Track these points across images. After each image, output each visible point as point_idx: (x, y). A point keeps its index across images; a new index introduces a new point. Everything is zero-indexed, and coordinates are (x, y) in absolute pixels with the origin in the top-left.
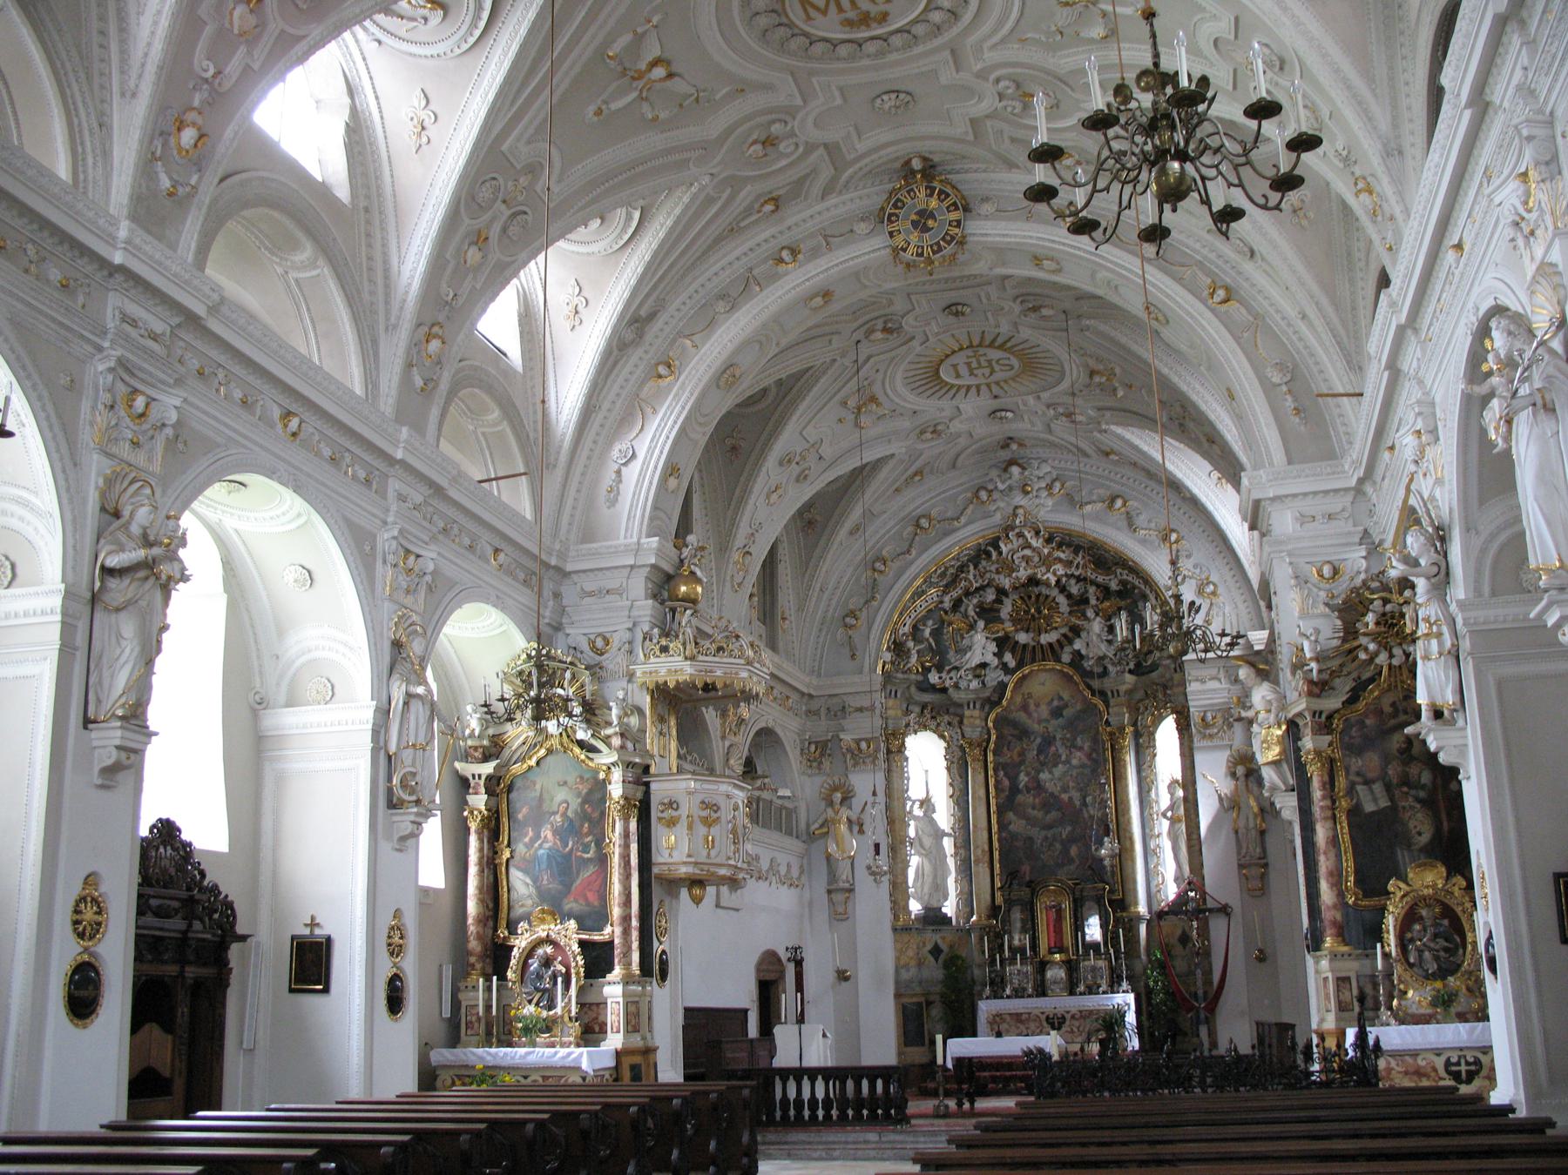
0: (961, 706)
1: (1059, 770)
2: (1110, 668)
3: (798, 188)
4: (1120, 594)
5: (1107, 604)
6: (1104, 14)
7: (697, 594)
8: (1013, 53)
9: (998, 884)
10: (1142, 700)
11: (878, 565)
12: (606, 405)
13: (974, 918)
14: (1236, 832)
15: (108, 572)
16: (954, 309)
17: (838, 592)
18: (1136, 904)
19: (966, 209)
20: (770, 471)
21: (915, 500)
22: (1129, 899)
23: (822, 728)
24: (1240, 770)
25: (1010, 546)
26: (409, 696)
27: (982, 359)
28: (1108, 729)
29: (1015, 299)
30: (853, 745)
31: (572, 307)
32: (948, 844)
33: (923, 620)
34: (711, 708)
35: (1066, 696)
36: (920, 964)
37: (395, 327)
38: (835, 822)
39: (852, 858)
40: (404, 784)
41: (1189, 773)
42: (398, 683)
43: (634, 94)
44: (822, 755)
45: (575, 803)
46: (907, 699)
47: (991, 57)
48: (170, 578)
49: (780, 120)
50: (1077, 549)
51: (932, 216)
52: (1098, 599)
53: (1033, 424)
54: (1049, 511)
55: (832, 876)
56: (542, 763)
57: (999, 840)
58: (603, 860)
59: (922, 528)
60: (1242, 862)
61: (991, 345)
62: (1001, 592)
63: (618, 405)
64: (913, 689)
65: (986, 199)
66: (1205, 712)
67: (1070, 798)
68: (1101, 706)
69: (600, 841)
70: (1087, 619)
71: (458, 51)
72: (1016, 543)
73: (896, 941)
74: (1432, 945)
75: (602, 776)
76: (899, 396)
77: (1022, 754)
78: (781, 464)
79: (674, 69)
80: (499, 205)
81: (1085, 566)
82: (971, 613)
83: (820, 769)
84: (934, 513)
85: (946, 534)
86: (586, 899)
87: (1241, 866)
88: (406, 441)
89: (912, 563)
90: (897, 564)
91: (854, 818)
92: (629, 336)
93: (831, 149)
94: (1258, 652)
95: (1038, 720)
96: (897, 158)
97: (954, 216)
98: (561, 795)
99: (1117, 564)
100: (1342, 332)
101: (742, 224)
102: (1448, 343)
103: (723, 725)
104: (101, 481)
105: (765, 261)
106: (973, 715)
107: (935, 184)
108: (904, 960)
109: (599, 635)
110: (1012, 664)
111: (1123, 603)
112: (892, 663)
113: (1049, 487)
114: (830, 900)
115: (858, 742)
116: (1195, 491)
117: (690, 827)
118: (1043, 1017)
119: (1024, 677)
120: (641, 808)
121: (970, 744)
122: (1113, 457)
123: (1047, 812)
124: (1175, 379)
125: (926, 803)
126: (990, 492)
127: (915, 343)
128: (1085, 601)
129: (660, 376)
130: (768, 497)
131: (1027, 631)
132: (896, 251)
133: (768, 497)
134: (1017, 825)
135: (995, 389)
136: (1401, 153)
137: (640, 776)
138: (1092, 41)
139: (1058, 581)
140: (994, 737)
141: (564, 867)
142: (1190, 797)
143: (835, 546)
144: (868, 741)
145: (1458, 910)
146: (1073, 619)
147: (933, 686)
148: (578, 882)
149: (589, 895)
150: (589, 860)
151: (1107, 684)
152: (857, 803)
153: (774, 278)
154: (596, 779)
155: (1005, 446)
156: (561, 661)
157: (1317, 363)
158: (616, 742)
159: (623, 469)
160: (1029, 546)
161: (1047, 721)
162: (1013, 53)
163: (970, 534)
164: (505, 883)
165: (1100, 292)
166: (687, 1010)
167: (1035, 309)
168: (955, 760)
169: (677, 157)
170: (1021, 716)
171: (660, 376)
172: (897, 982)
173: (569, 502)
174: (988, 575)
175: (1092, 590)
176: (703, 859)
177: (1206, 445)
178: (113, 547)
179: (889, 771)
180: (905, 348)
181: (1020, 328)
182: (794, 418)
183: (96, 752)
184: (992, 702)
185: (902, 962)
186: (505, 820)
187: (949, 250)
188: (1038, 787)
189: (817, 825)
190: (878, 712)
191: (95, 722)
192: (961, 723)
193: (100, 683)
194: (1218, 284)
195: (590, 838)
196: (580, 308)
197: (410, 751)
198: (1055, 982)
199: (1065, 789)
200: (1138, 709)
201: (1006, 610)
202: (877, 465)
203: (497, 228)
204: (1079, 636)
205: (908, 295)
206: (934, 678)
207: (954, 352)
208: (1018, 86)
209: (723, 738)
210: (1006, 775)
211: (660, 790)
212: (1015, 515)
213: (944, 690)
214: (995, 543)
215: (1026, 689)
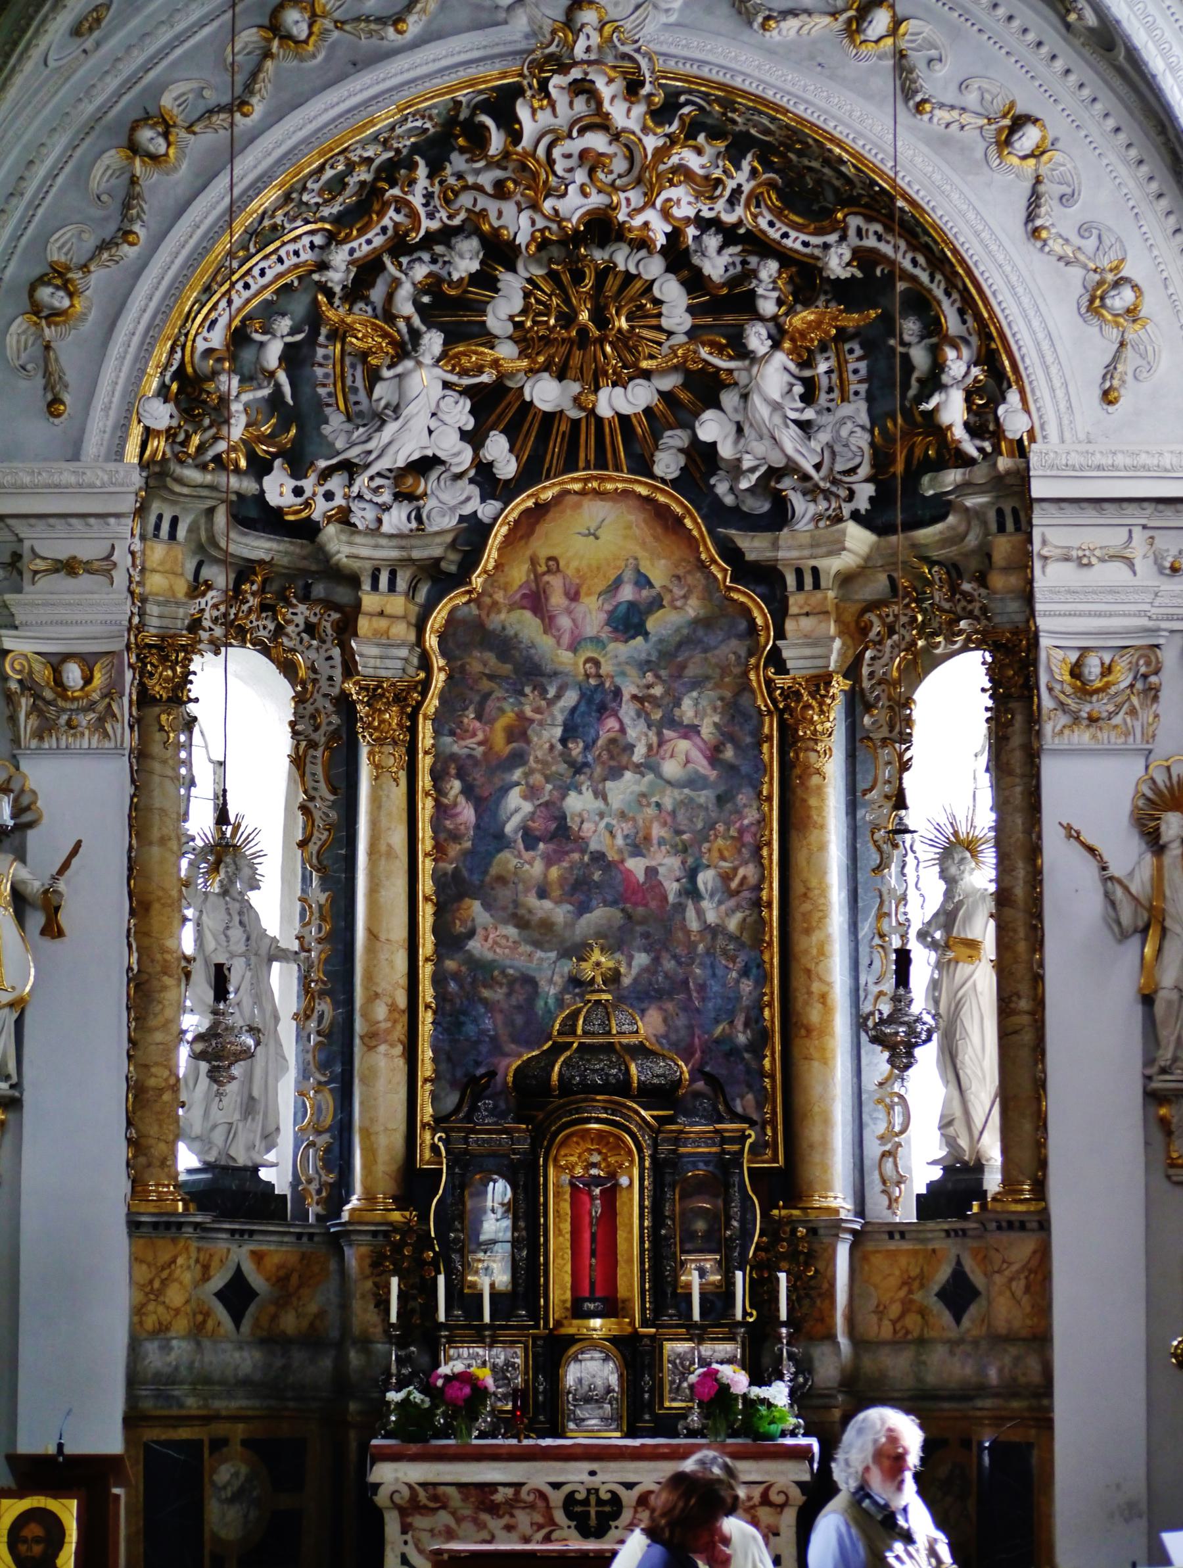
0: (354, 581)
2: (798, 502)
4: (842, 291)
5: (803, 317)
9: (426, 1111)
10: (873, 606)
11: (146, 135)
13: (354, 1202)
18: (828, 1187)
25: (545, 118)
28: (780, 681)
30: (43, 674)
33: (269, 312)
35: (658, 573)
36: (197, 1332)
46: (200, 548)
50: (737, 149)
52: (780, 302)
59: (287, 37)
64: (221, 518)
66: (1084, 650)
67: (651, 872)
70: (743, 353)
72: (568, 109)
77: (519, 732)
81: (756, 199)
82: (405, 307)
85: (359, 64)
89: (253, 137)
91: (35, 885)
99: (849, 202)
110: (507, 468)
111: (852, 320)
112: (170, 434)
115: (56, 662)
118: (557, 1497)
119: (540, 511)
123: (583, 908)
128: (746, 304)
131: (561, 377)
139: (675, 236)
140: (439, 680)
142: (1019, 892)
143: (29, 66)
144: (87, 661)
146: (704, 352)
147: (279, 511)
160: (601, 123)
161: (596, 641)
168: (320, 737)
170: (525, 625)
172: (133, 1381)
174: (466, 200)
185: (150, 1322)
190: (120, 577)
192: (346, 628)
198: (588, 1400)
199: (638, 846)
200: (865, 630)
204: (718, 406)
210: (468, 791)
213: (307, 530)
215: (543, 544)
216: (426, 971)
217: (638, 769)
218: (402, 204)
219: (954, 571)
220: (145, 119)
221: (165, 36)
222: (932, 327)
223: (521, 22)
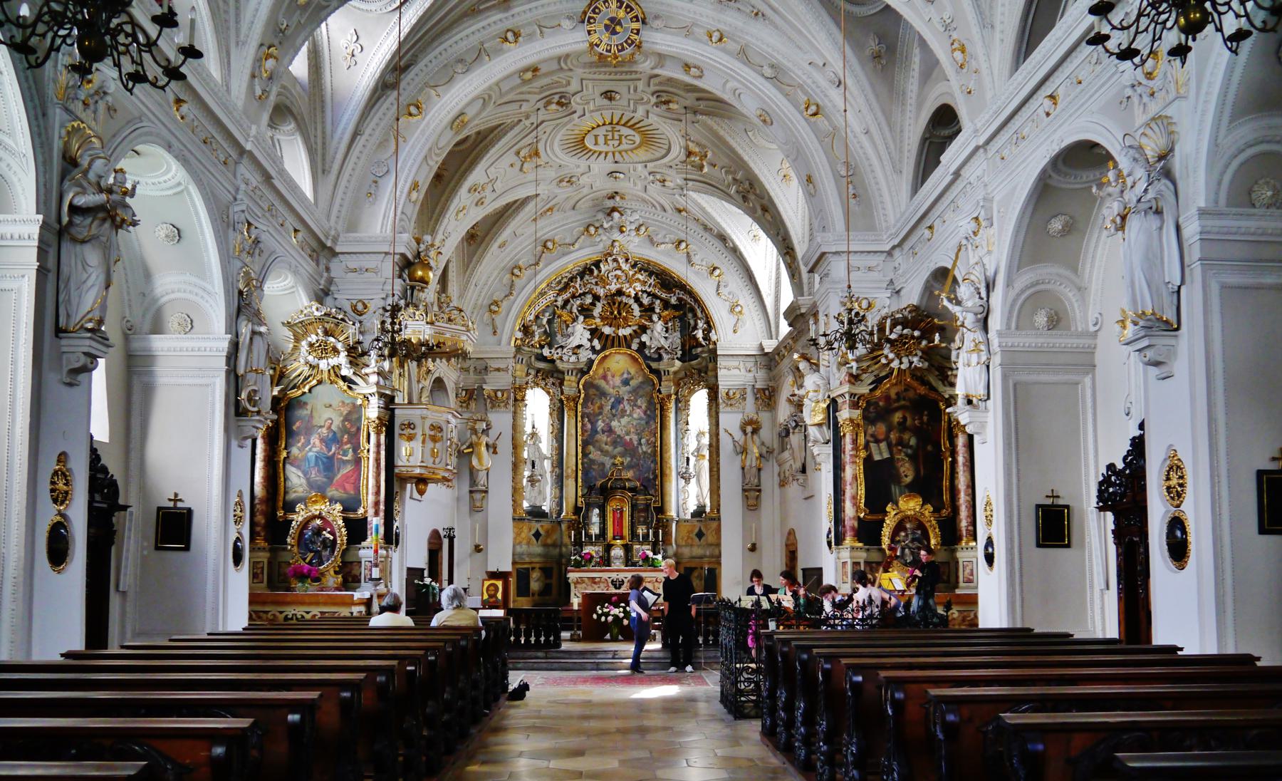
0: (563, 373)
1: (624, 420)
2: (665, 356)
4: (675, 307)
7: (428, 277)
9: (580, 493)
10: (681, 379)
11: (516, 271)
12: (368, 131)
14: (743, 469)
15: (74, 209)
16: (608, 95)
17: (487, 287)
19: (644, 22)
20: (463, 197)
21: (547, 228)
22: (667, 506)
23: (471, 380)
24: (749, 429)
26: (254, 333)
29: (653, 94)
30: (493, 394)
31: (350, 51)
32: (547, 465)
33: (544, 311)
34: (444, 360)
35: (633, 371)
36: (528, 543)
37: (244, 43)
38: (479, 444)
39: (487, 470)
40: (250, 399)
41: (714, 428)
45: (337, 423)
48: (123, 221)
50: (651, 274)
51: (619, 23)
53: (635, 184)
54: (636, 246)
55: (473, 482)
56: (313, 390)
57: (582, 464)
58: (357, 461)
60: (746, 487)
61: (624, 125)
62: (596, 298)
63: (377, 132)
64: (533, 358)
65: (657, 17)
68: (656, 381)
69: (356, 448)
70: (652, 321)
73: (514, 527)
74: (911, 545)
75: (359, 402)
77: (601, 407)
78: (469, 191)
81: (655, 286)
82: (575, 310)
83: (467, 407)
84: (557, 239)
85: (564, 255)
86: (345, 489)
87: (744, 490)
88: (255, 137)
90: (530, 272)
91: (491, 443)
92: (390, 79)
94: (767, 354)
95: (613, 386)
97: (635, 25)
98: (327, 414)
99: (676, 287)
100: (892, 146)
101: (481, 8)
103: (419, 373)
104: (63, 132)
106: (570, 380)
109: (360, 301)
110: (598, 347)
111: (677, 314)
113: (638, 229)
114: (472, 499)
115: (496, 392)
116: (738, 243)
117: (424, 442)
118: (610, 581)
119: (606, 357)
120: (388, 424)
121: (568, 399)
122: (684, 213)
123: (615, 448)
124: (752, 165)
126: (597, 228)
127: (575, 116)
129: (410, 115)
132: (592, 45)
134: (595, 454)
135: (618, 156)
136: (992, 26)
137: (389, 402)
139: (636, 294)
140: (582, 396)
141: (328, 465)
144: (503, 391)
145: (927, 525)
148: (339, 476)
149: (347, 486)
150: (348, 461)
151: (662, 366)
152: (493, 433)
153: (499, 52)
154: (354, 405)
155: (612, 197)
156: (334, 317)
157: (870, 165)
158: (374, 378)
160: (620, 268)
163: (582, 255)
164: (282, 475)
165: (726, 97)
166: (409, 569)
170: (602, 383)
171: (410, 115)
173: (338, 201)
174: (589, 286)
175: (658, 302)
176: (430, 465)
177: (759, 212)
178: (78, 189)
179: (515, 412)
180: (568, 118)
181: (650, 115)
182: (485, 159)
183: (65, 357)
184: (583, 372)
186: (283, 431)
187: (629, 50)
188: (610, 430)
190: (510, 372)
191: (66, 331)
192: (561, 384)
193: (69, 300)
194: (812, 101)
195: (349, 446)
196: (355, 53)
197: (254, 374)
199: (628, 433)
201: (597, 311)
202: (526, 201)
205: (582, 80)
206: (546, 352)
207: (598, 126)
209: (419, 382)
211: (401, 415)
212: (612, 245)
213: (553, 361)
214: (597, 264)
216: (580, 462)
217: (629, 416)
218: (574, 287)
219: (700, 371)
220: (515, 267)
221: (520, 248)
222: (695, 315)
223: (601, 245)
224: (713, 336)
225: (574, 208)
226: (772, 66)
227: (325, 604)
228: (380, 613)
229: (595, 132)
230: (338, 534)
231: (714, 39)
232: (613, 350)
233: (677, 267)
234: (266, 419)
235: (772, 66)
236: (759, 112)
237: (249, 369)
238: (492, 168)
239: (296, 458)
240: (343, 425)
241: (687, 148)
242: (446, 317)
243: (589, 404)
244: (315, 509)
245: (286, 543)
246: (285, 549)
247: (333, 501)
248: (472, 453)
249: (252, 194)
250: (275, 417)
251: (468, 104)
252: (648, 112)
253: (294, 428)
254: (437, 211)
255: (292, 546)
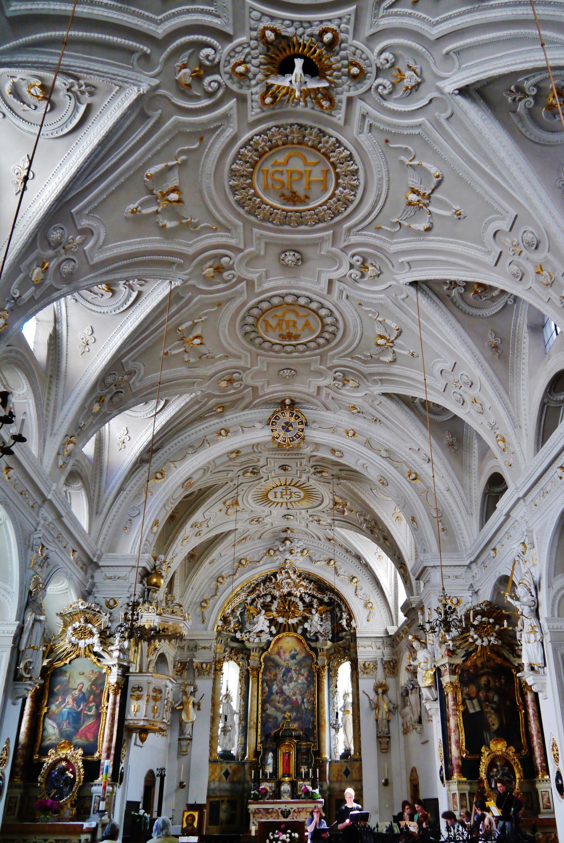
0: (249, 650)
1: (292, 685)
2: (320, 638)
3: (234, 404)
4: (327, 604)
5: (321, 608)
6: (394, 352)
8: (347, 361)
9: (259, 741)
10: (332, 654)
11: (220, 579)
12: (128, 488)
13: (247, 757)
16: (284, 468)
19: (306, 425)
20: (187, 530)
21: (242, 551)
22: (323, 751)
23: (185, 655)
26: (35, 620)
27: (288, 491)
29: (312, 467)
30: (199, 665)
31: (122, 440)
32: (236, 718)
33: (238, 607)
34: (167, 641)
36: (220, 781)
39: (193, 722)
40: (26, 668)
41: (355, 690)
42: (30, 613)
43: (183, 349)
44: (183, 669)
45: (87, 686)
47: (336, 362)
49: (238, 372)
51: (291, 425)
53: (300, 523)
57: (262, 717)
62: (274, 598)
63: (135, 488)
64: (229, 640)
65: (314, 422)
67: (296, 699)
68: (314, 656)
70: (311, 613)
71: (114, 313)
73: (210, 767)
75: (104, 671)
76: (248, 503)
77: (276, 675)
78: (192, 527)
79: (204, 341)
80: (113, 386)
81: (313, 589)
82: (259, 606)
83: (181, 675)
84: (248, 558)
85: (253, 568)
88: (54, 491)
91: (196, 701)
92: (146, 457)
93: (255, 389)
95: (284, 660)
96: (279, 398)
97: (301, 427)
99: (328, 590)
102: (549, 507)
103: (149, 650)
105: (212, 433)
106: (254, 655)
107: (294, 412)
108: (213, 777)
109: (112, 599)
110: (274, 632)
111: (328, 608)
113: (302, 552)
115: (202, 664)
116: (368, 561)
117: (148, 701)
118: (280, 811)
119: (279, 639)
121: (252, 669)
122: (332, 541)
123: (285, 705)
124: (376, 510)
125: (227, 696)
127: (263, 480)
129: (157, 478)
130: (182, 542)
132: (274, 438)
133: (182, 542)
134: (271, 711)
135: (289, 504)
137: (125, 671)
138: (385, 362)
139: (301, 595)
140: (263, 667)
144: (207, 663)
151: (318, 645)
152: (198, 694)
153: (216, 441)
156: (93, 610)
157: (452, 510)
158: (116, 654)
159: (133, 519)
160: (290, 578)
162: (347, 361)
165: (358, 469)
167: (320, 472)
169: (191, 380)
170: (277, 658)
171: (157, 478)
173: (104, 532)
175: (315, 600)
176: (151, 719)
177: (382, 540)
179: (215, 679)
180: (257, 482)
184: (263, 650)
187: (297, 441)
188: (281, 692)
189: (177, 705)
190: (213, 650)
192: (248, 658)
194: (412, 471)
197: (31, 650)
199: (294, 694)
200: (330, 658)
201: (274, 607)
202: (228, 533)
203: (109, 396)
206: (238, 635)
207: (277, 486)
208: (344, 375)
209: (148, 656)
210: (267, 685)
211: (133, 680)
212: (285, 562)
213: (243, 642)
214: (275, 575)
216: (260, 716)
218: (259, 590)
219: (344, 649)
220: (220, 577)
221: (223, 564)
222: (341, 610)
223: (278, 562)
224: (353, 624)
225: (260, 538)
226: (386, 451)
227: (60, 833)
228: (102, 840)
229: (275, 490)
230: (77, 774)
231: (350, 435)
232: (284, 634)
233: (328, 577)
234: (35, 683)
235: (386, 450)
236: (379, 478)
237: (28, 646)
238: (207, 512)
239: (54, 713)
240: (91, 688)
241: (334, 500)
242: (170, 610)
243: (268, 673)
244: (62, 753)
245: (37, 781)
246: (36, 786)
247: (76, 747)
248: (182, 709)
249: (47, 527)
250: (42, 682)
251: (193, 473)
252: (309, 478)
253: (55, 690)
254: (170, 538)
255: (41, 784)
